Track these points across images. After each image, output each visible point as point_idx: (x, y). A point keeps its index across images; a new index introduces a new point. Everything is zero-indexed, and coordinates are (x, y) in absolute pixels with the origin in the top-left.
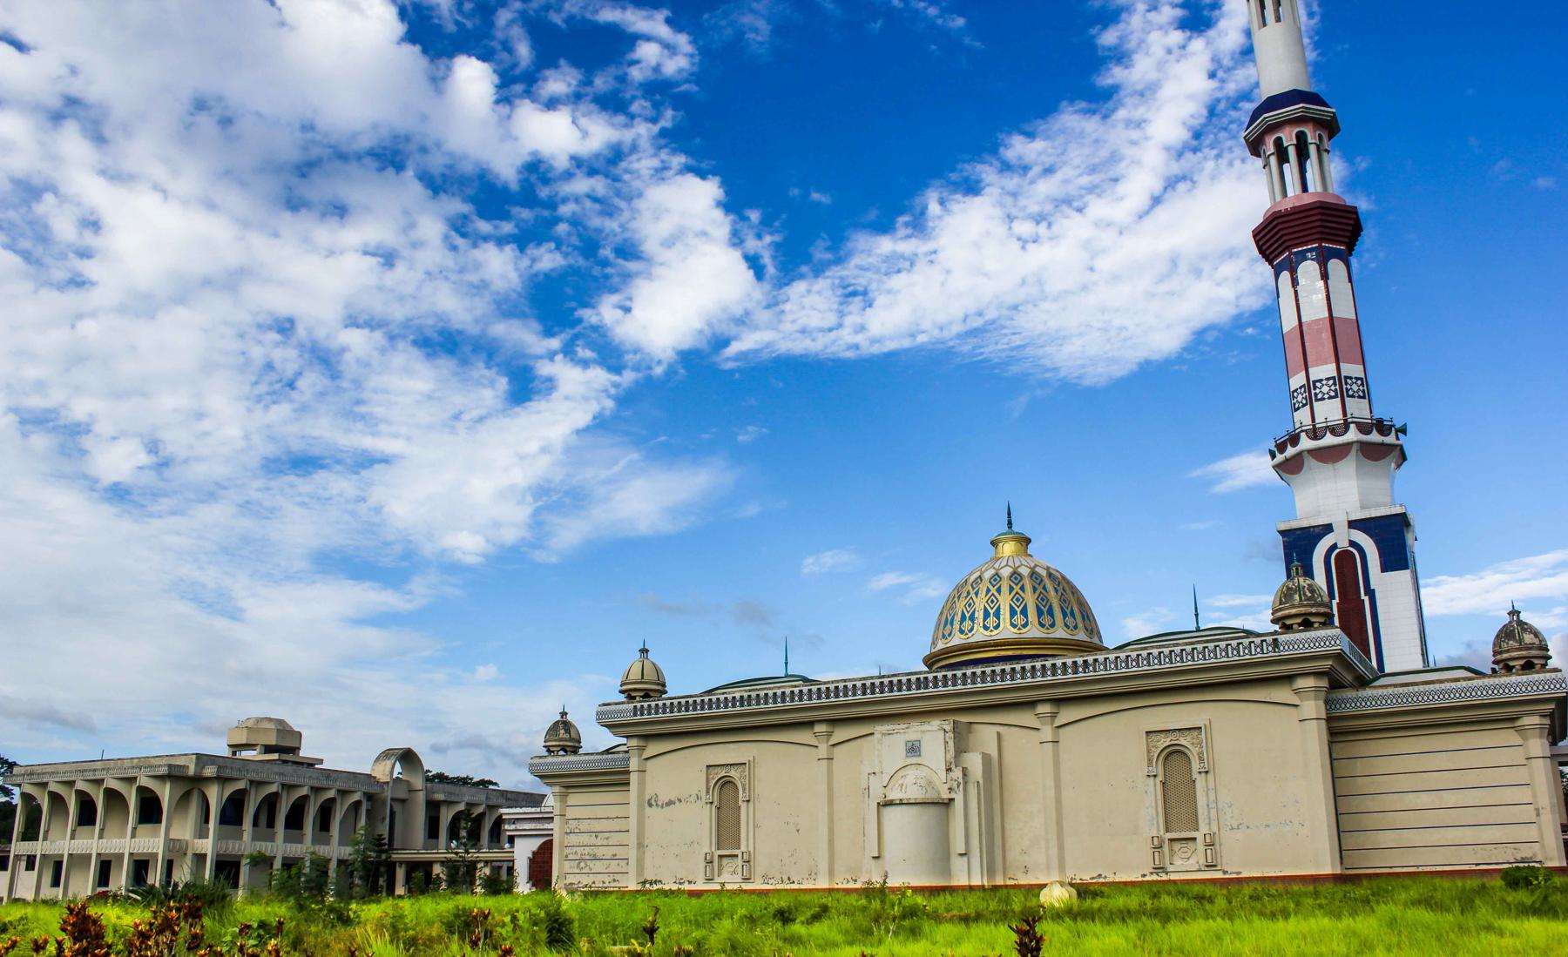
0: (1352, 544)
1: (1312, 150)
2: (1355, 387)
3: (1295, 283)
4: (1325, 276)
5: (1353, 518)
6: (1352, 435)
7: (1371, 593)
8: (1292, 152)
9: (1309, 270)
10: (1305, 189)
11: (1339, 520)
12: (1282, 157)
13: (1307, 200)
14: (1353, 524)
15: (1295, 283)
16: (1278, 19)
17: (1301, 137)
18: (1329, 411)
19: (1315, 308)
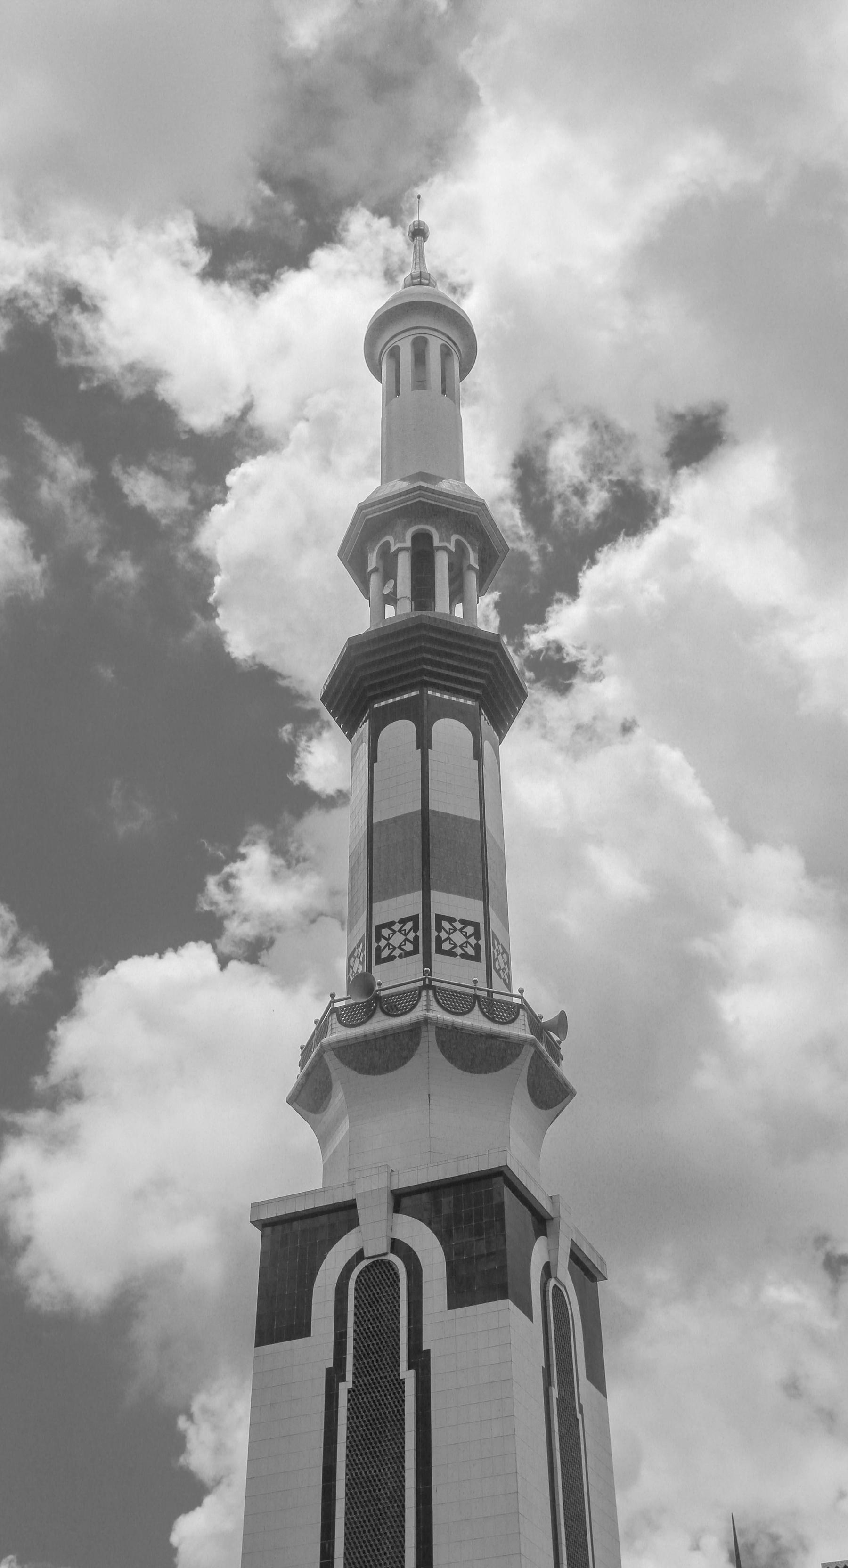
0: (396, 1246)
5: (403, 1182)
11: (371, 1191)
14: (401, 1200)
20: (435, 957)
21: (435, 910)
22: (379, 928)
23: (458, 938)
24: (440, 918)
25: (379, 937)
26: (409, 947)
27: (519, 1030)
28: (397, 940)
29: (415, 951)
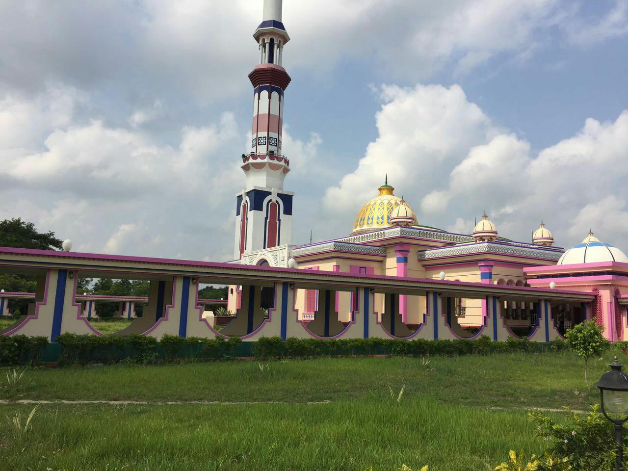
2: (273, 142)
3: (259, 98)
4: (270, 97)
8: (267, 46)
9: (264, 94)
13: (270, 66)
15: (259, 98)
17: (272, 41)
19: (264, 110)
20: (269, 146)
21: (269, 136)
22: (259, 138)
23: (273, 142)
24: (270, 137)
25: (259, 140)
26: (264, 143)
28: (262, 141)
29: (265, 144)
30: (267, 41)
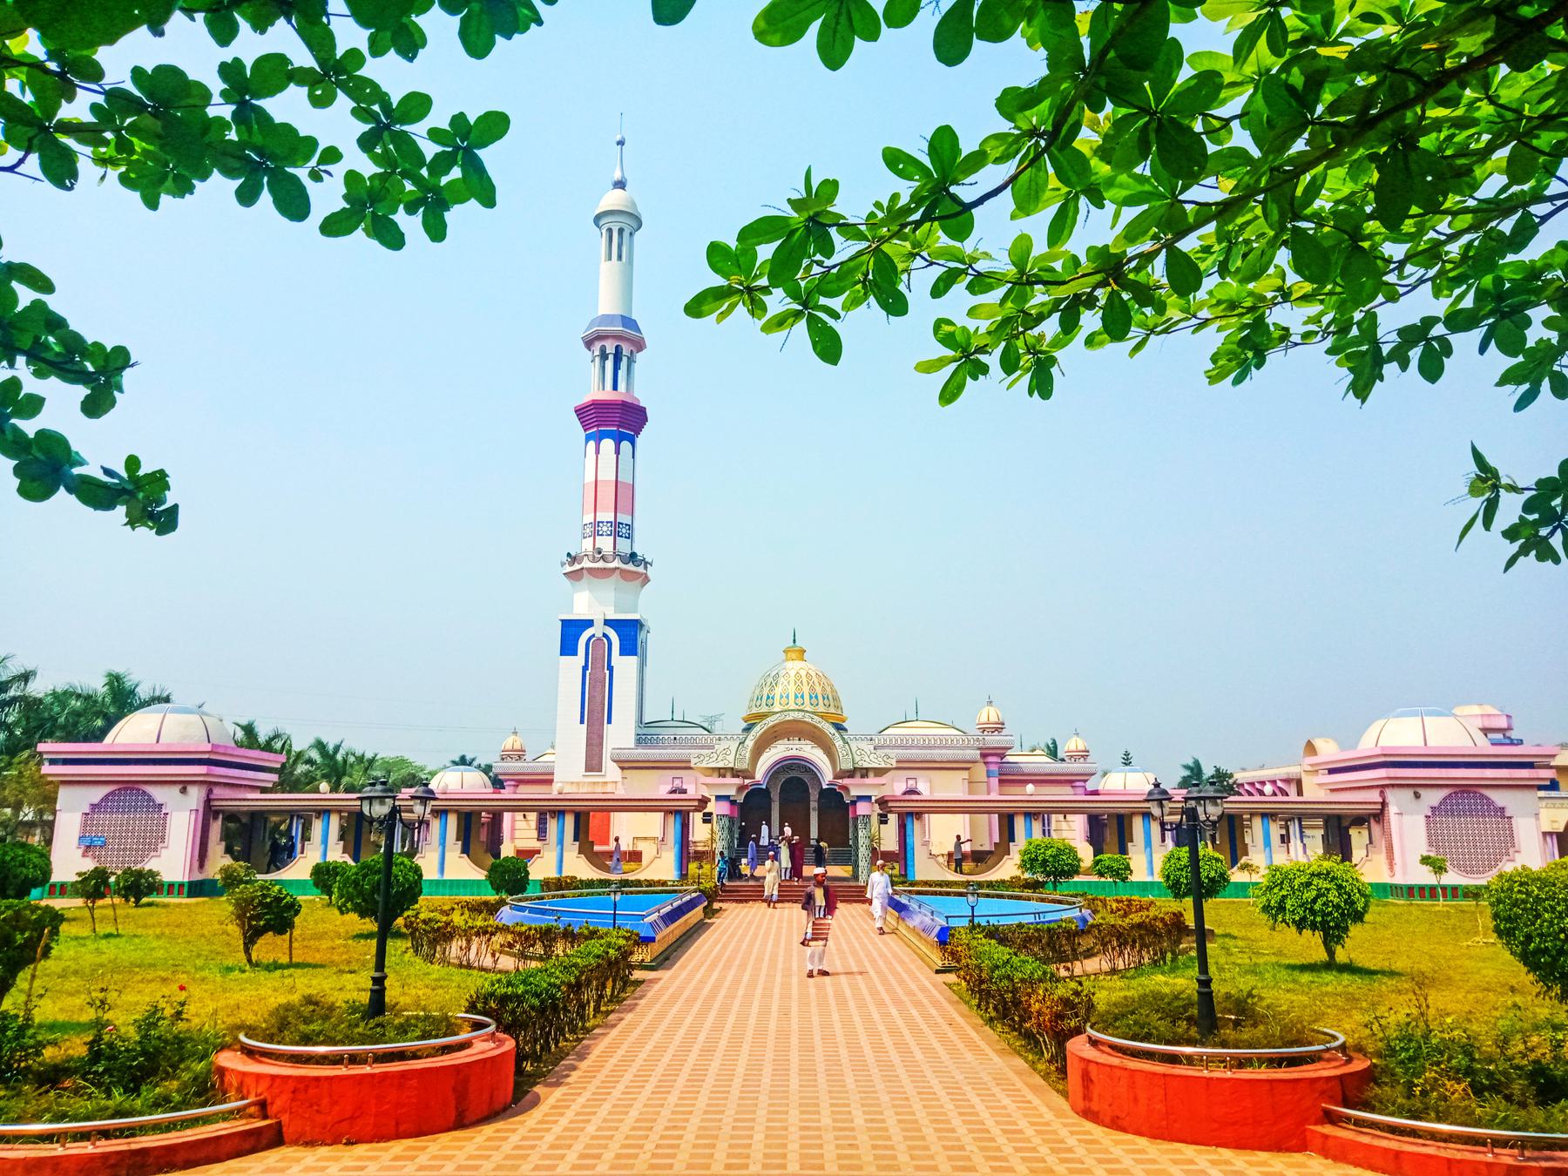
0: (605, 635)
1: (625, 359)
3: (598, 451)
4: (617, 452)
6: (616, 564)
7: (611, 669)
9: (608, 445)
10: (615, 387)
12: (604, 356)
15: (598, 451)
16: (620, 257)
18: (606, 544)
19: (607, 474)
27: (641, 569)
30: (610, 349)
